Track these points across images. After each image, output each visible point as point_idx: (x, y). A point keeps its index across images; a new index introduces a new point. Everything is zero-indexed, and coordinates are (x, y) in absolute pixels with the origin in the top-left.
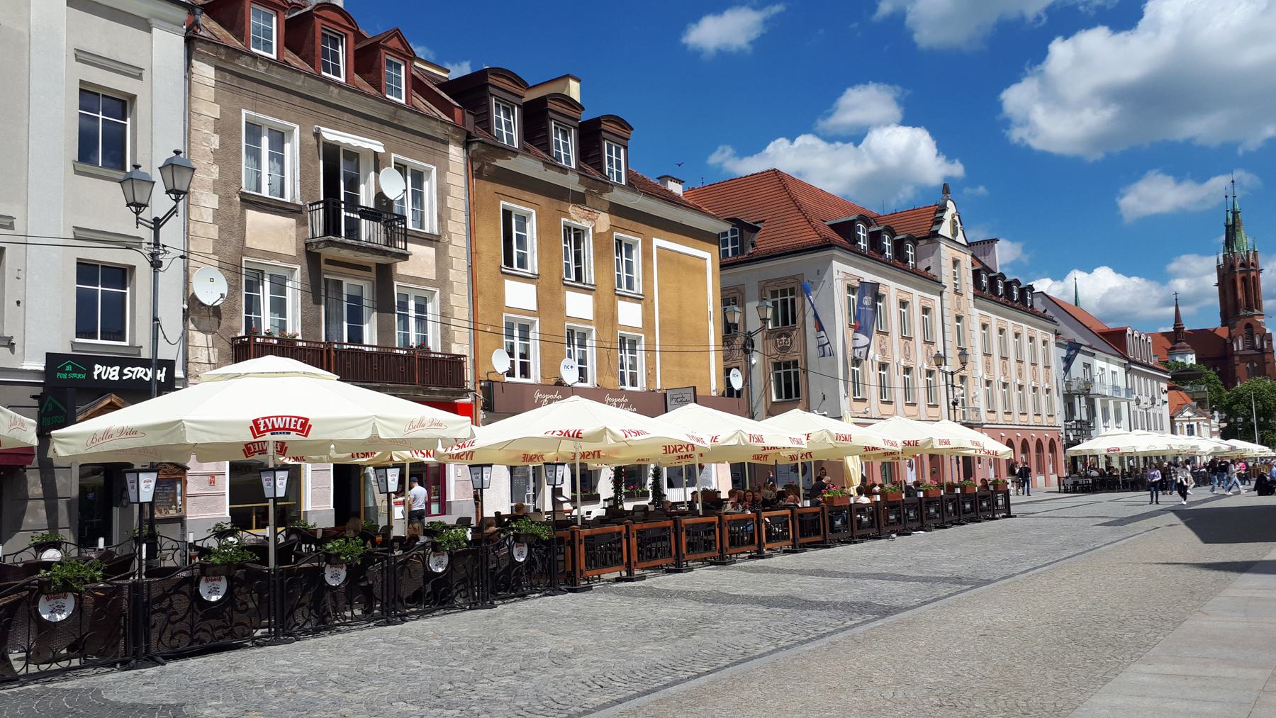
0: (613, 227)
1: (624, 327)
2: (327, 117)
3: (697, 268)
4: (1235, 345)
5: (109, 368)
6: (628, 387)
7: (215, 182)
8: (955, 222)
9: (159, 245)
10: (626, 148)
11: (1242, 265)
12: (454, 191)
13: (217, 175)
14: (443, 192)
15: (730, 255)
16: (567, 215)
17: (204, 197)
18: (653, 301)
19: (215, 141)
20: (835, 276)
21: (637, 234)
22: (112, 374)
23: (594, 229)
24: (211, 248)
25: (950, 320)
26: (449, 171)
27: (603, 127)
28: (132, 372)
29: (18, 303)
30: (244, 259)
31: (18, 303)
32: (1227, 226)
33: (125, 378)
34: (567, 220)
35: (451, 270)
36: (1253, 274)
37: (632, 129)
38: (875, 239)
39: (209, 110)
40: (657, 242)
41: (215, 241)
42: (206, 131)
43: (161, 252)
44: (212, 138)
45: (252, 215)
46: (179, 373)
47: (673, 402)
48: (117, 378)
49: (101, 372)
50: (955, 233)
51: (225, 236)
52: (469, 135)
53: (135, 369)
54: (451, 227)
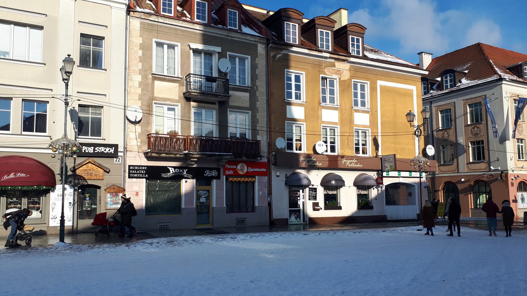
0: (352, 77)
1: (358, 126)
2: (195, 39)
3: (408, 94)
5: (89, 148)
6: (361, 154)
7: (140, 70)
9: (67, 96)
10: (363, 38)
12: (259, 65)
13: (141, 67)
14: (254, 67)
15: (449, 87)
17: (135, 76)
18: (376, 111)
19: (140, 53)
20: (504, 95)
21: (367, 79)
22: (90, 150)
23: (340, 79)
24: (138, 97)
26: (257, 58)
27: (348, 29)
28: (99, 149)
29: (54, 122)
30: (154, 102)
31: (54, 122)
33: (96, 152)
35: (257, 102)
37: (366, 29)
39: (137, 40)
40: (380, 83)
41: (140, 95)
42: (136, 49)
43: (69, 98)
44: (139, 52)
45: (157, 83)
46: (121, 149)
48: (92, 152)
49: (85, 149)
51: (145, 92)
52: (268, 40)
53: (100, 148)
54: (258, 83)
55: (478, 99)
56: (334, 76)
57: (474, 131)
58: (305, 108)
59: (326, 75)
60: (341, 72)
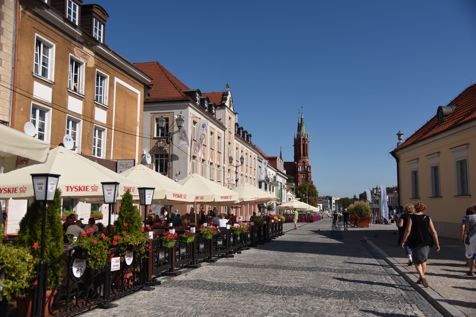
0: (96, 66)
3: (133, 97)
4: (299, 169)
6: (96, 156)
8: (231, 101)
10: (104, 25)
11: (303, 139)
16: (73, 52)
18: (112, 110)
21: (108, 73)
23: (86, 64)
25: (227, 144)
32: (299, 124)
34: (72, 55)
36: (306, 143)
37: (108, 16)
38: (202, 101)
40: (117, 80)
47: (121, 167)
50: (230, 106)
55: (166, 115)
56: (81, 60)
57: (160, 144)
58: (53, 89)
59: (75, 55)
60: (87, 56)
